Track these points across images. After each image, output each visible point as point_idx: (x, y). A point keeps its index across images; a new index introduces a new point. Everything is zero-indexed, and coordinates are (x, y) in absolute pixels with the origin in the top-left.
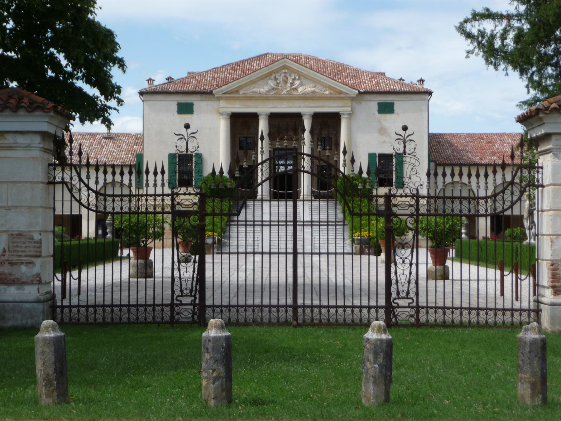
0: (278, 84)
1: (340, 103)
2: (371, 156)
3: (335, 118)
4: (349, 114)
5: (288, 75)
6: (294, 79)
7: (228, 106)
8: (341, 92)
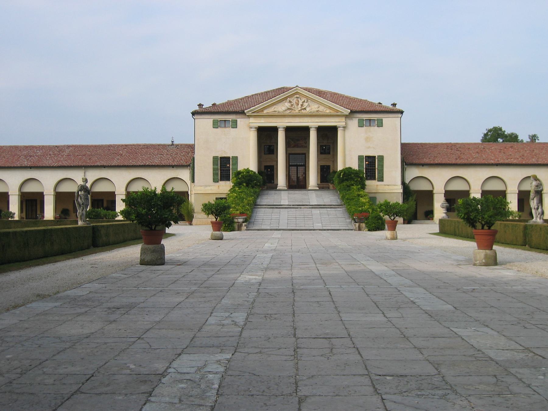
2: (360, 158)
3: (334, 130)
4: (344, 127)
5: (299, 100)
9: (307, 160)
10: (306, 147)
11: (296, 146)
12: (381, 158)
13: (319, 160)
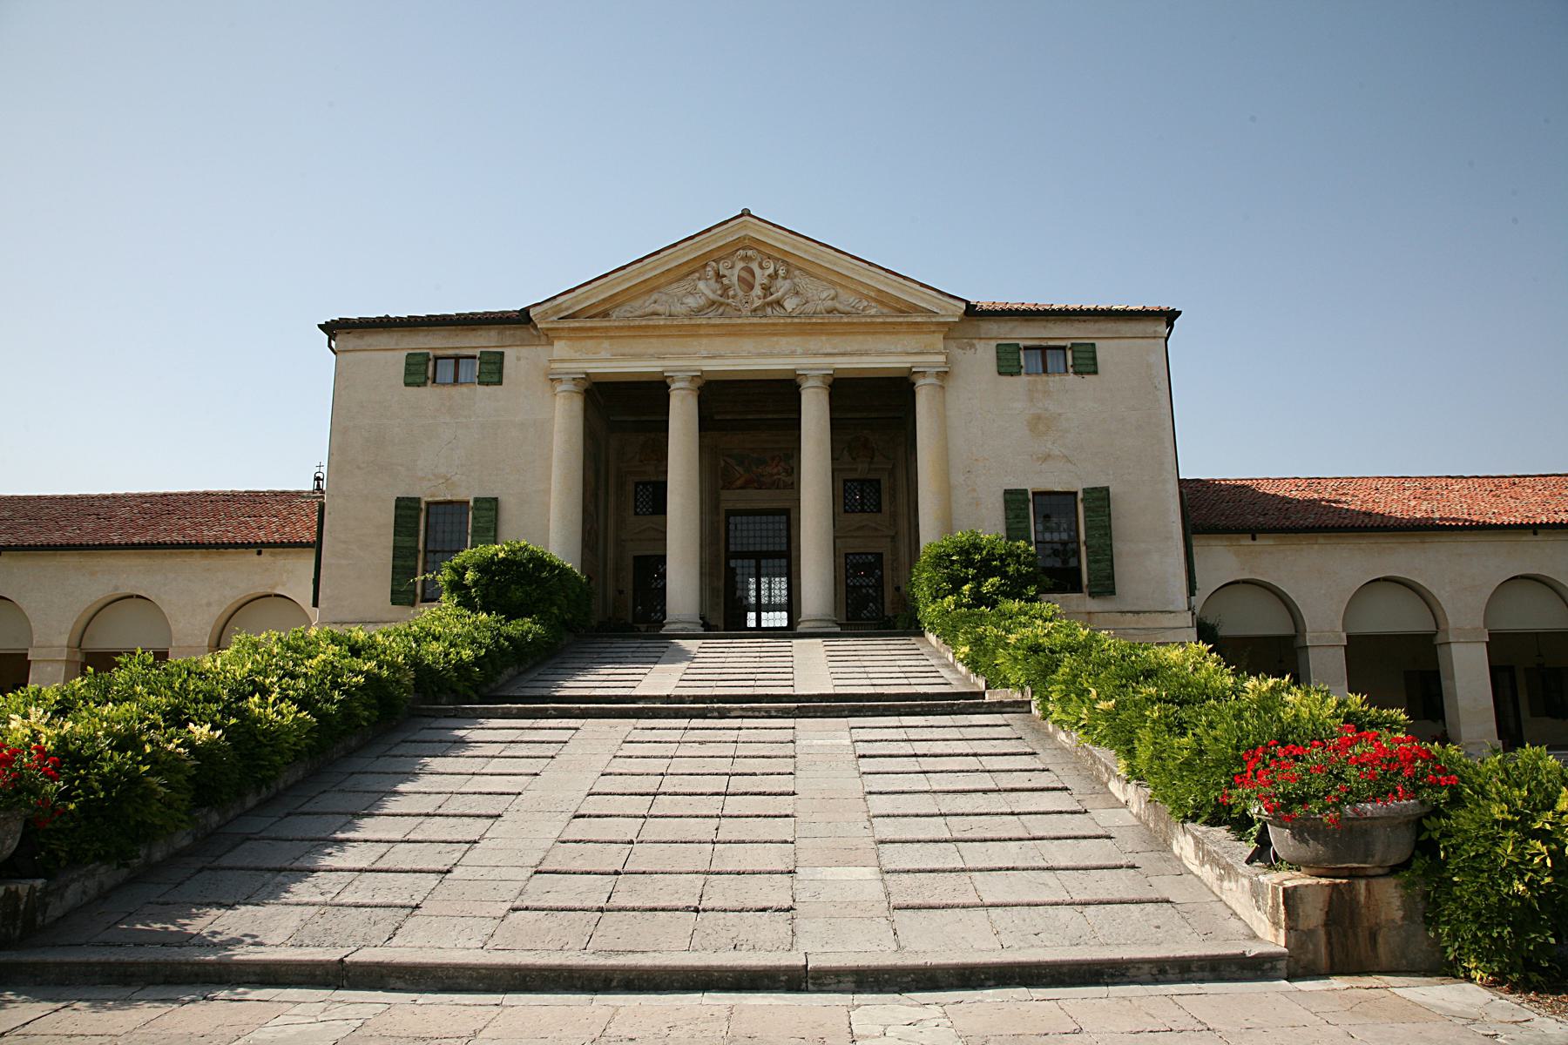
0: (725, 293)
1: (911, 342)
2: (1014, 500)
4: (943, 375)
5: (755, 266)
6: (774, 276)
7: (577, 356)
8: (916, 309)
9: (793, 532)
12: (1100, 499)
13: (840, 533)
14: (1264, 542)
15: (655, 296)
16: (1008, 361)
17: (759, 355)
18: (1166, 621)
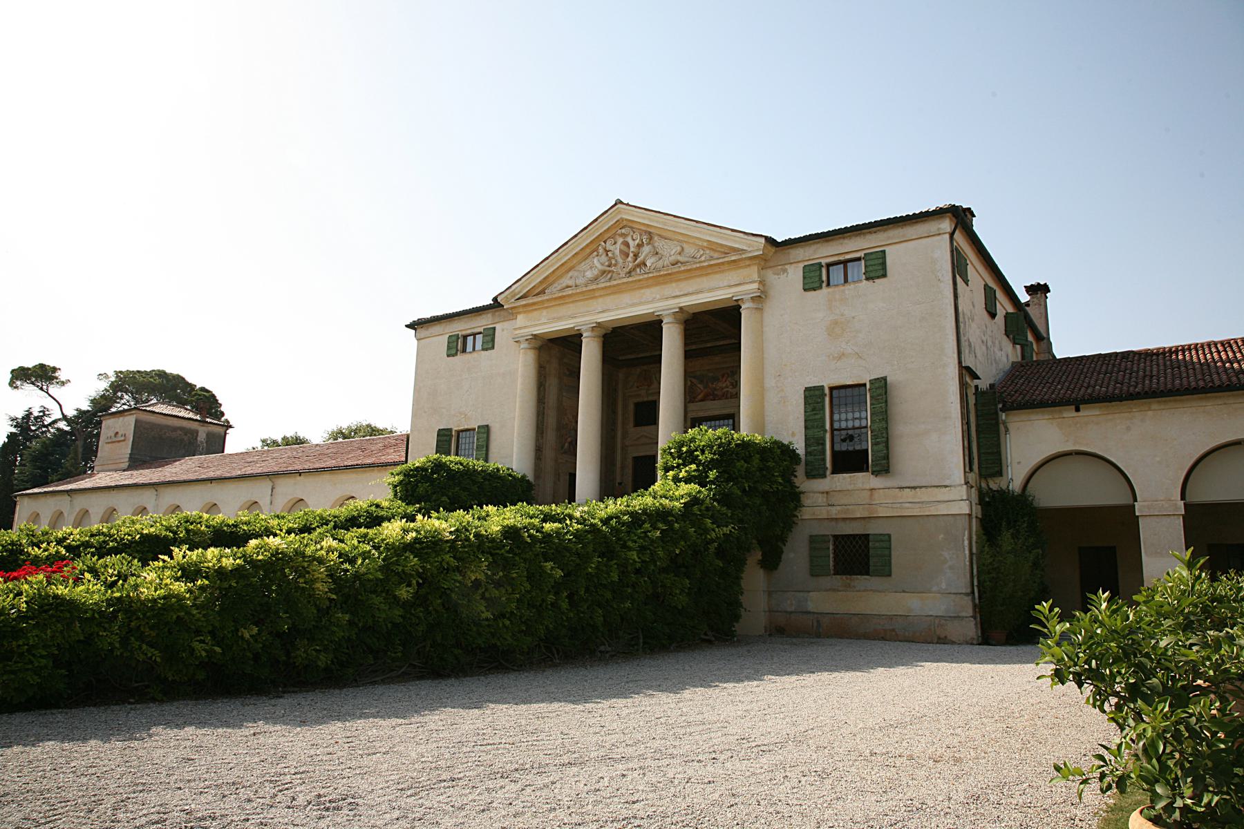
1: (733, 276)
2: (813, 396)
5: (629, 240)
6: (640, 246)
10: (725, 396)
11: (712, 396)
14: (1088, 412)
15: (570, 274)
16: (814, 279)
17: (633, 305)
18: (942, 494)
